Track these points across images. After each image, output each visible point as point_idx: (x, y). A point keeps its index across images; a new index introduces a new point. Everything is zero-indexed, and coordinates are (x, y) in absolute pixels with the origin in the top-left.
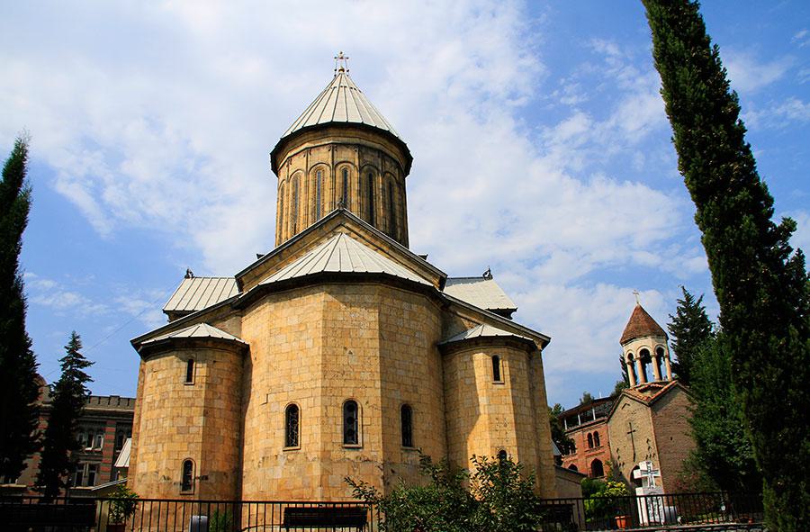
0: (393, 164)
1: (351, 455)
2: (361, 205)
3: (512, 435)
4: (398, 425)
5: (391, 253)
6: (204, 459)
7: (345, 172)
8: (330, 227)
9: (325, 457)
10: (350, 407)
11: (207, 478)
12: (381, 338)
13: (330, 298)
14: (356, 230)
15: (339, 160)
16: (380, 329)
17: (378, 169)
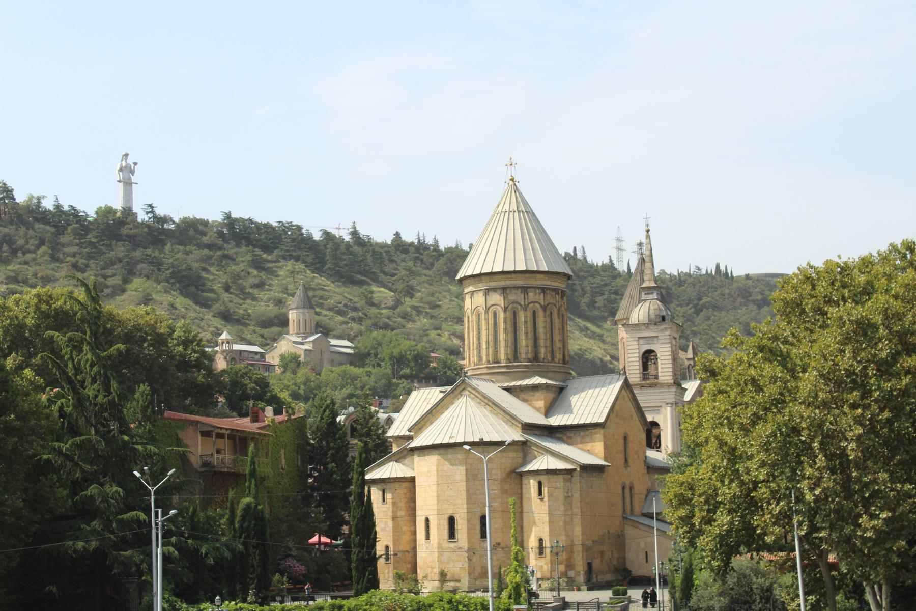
0: (538, 291)
1: (452, 545)
2: (506, 341)
3: (547, 529)
4: (478, 527)
5: (494, 407)
6: (394, 545)
7: (495, 314)
8: (458, 390)
9: (440, 547)
10: (452, 521)
11: (396, 554)
12: (468, 480)
13: (439, 457)
14: (474, 392)
15: (492, 303)
16: (467, 474)
17: (521, 305)
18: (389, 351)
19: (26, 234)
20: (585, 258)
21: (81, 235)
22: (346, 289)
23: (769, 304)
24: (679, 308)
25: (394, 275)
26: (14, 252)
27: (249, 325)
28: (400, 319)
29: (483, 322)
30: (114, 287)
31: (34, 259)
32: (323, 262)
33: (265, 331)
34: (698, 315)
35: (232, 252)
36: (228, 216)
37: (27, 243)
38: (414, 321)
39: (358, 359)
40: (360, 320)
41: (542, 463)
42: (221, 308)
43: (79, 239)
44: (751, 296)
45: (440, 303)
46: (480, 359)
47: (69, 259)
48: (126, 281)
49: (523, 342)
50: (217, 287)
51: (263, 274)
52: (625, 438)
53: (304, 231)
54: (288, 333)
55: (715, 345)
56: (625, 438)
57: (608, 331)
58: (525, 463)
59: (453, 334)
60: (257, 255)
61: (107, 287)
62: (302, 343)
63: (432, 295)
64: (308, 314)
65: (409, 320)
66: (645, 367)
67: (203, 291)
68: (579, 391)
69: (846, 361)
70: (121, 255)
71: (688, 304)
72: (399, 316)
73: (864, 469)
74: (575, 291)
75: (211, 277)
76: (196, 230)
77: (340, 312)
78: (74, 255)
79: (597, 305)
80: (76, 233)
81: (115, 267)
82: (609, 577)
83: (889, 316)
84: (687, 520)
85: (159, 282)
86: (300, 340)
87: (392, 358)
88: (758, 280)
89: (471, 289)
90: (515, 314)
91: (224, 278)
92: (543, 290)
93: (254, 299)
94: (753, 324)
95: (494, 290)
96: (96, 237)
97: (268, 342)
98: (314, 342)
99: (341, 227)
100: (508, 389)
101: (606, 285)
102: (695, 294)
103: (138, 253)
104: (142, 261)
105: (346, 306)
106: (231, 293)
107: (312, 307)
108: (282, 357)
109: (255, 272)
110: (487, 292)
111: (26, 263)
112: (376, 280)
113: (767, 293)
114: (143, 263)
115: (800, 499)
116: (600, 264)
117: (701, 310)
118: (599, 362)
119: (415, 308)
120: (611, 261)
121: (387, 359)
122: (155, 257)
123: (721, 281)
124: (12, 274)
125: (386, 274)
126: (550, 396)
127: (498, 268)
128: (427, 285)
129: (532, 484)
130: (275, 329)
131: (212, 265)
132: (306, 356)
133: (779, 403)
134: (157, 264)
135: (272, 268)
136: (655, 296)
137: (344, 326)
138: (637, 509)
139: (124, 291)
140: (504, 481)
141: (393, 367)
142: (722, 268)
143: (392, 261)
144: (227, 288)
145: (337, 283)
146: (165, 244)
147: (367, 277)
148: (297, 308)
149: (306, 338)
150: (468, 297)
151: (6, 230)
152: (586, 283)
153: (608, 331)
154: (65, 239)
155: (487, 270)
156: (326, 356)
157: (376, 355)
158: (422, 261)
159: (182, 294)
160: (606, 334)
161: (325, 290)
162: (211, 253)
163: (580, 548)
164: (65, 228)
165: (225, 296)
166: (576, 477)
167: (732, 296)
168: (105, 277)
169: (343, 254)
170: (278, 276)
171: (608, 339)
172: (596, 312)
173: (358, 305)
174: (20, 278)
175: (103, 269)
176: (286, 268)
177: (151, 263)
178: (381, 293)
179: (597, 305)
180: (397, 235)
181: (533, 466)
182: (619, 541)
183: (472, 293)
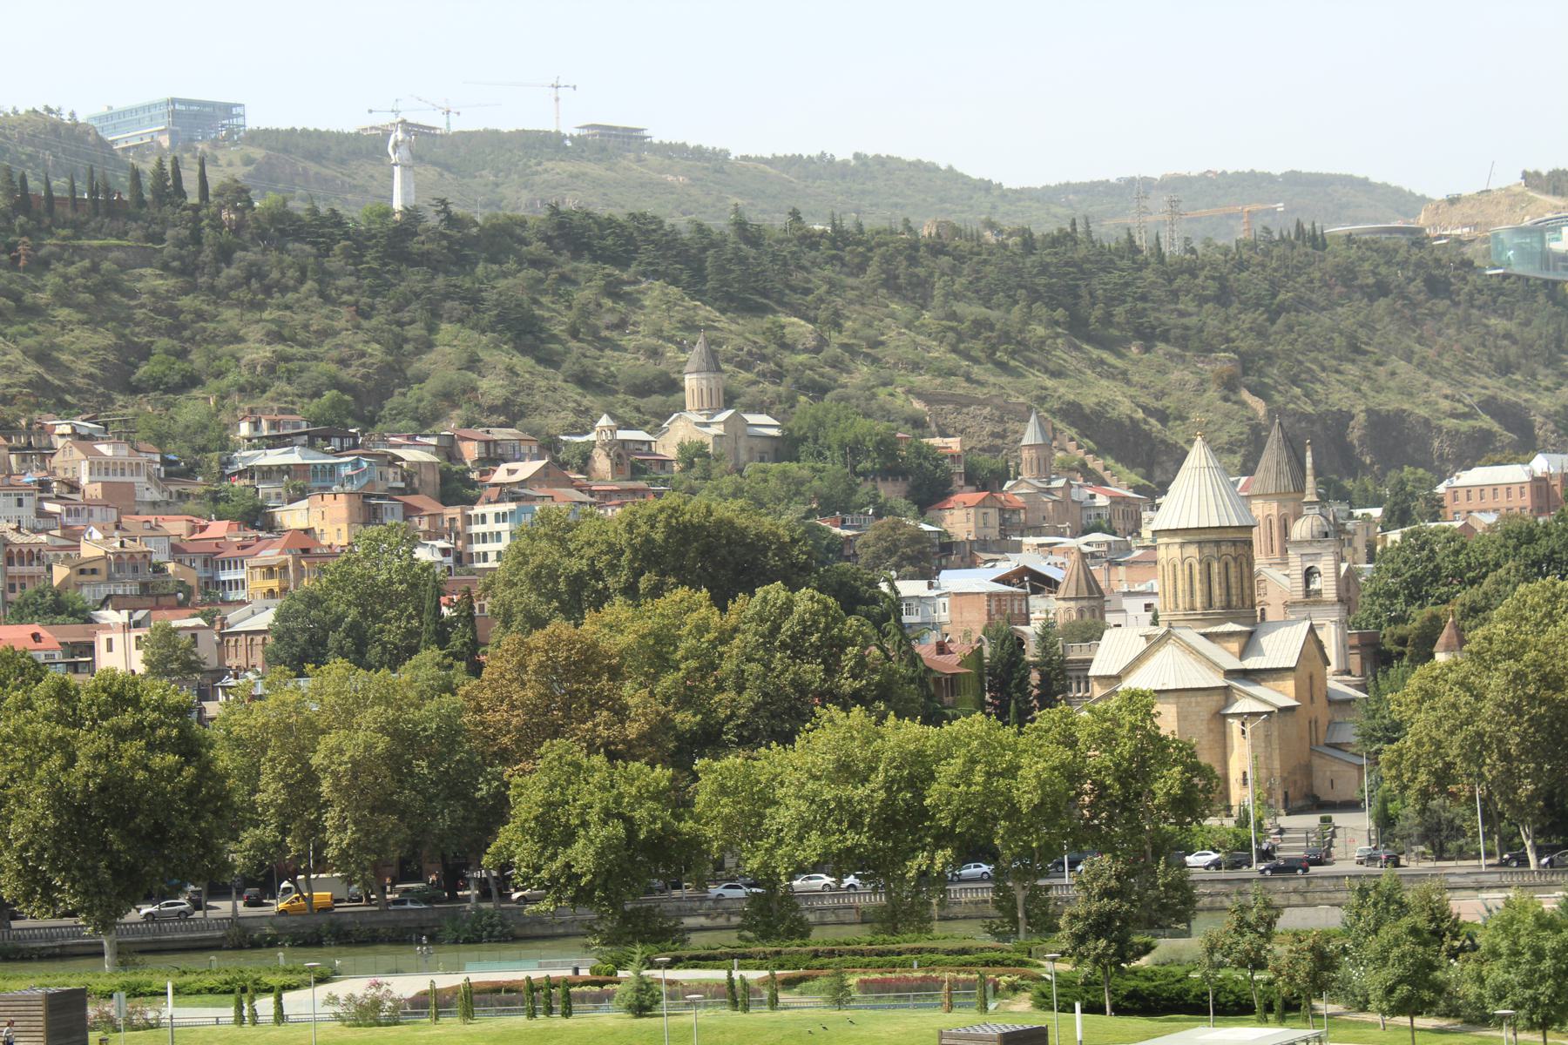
18: (838, 436)
19: (280, 261)
20: (1089, 233)
21: (354, 256)
22: (750, 326)
23: (1385, 295)
24: (1242, 316)
25: (807, 292)
26: (267, 291)
27: (617, 392)
28: (827, 369)
29: (1179, 573)
30: (415, 340)
31: (298, 300)
32: (699, 274)
33: (642, 402)
34: (1273, 322)
35: (567, 268)
36: (555, 210)
37: (283, 274)
38: (849, 372)
39: (786, 448)
40: (777, 376)
41: (1243, 706)
42: (576, 367)
43: (355, 264)
44: (1356, 278)
45: (883, 338)
46: (1177, 606)
47: (346, 298)
48: (432, 329)
49: (1216, 590)
50: (557, 330)
51: (621, 306)
52: (1311, 677)
53: (667, 227)
54: (683, 408)
55: (1303, 376)
56: (1311, 677)
57: (1135, 363)
58: (1227, 705)
59: (909, 391)
60: (609, 275)
61: (406, 340)
62: (707, 425)
63: (870, 326)
64: (716, 381)
65: (842, 370)
66: (1307, 583)
67: (543, 341)
68: (1267, 633)
69: (1508, 697)
70: (419, 287)
71: (1257, 305)
72: (826, 362)
73: (1522, 762)
74: (1078, 297)
75: (547, 314)
76: (512, 236)
77: (744, 365)
78: (350, 291)
79: (1116, 319)
80: (347, 253)
81: (412, 307)
82: (1300, 803)
83: (1537, 665)
84: (1399, 777)
85: (483, 332)
86: (703, 419)
87: (842, 445)
88: (1366, 242)
89: (1165, 540)
90: (1209, 565)
91: (569, 317)
92: (1234, 543)
93: (617, 347)
94: (1362, 334)
95: (1190, 543)
96: (375, 259)
97: (657, 420)
98: (725, 422)
99: (562, 83)
100: (1205, 635)
101: (1127, 284)
102: (1266, 285)
103: (440, 282)
104: (447, 296)
105: (750, 353)
106: (580, 341)
107: (719, 370)
108: (682, 448)
109: (608, 303)
110: (1182, 545)
111: (288, 307)
112: (780, 303)
113: (1383, 270)
114: (453, 299)
115: (1481, 776)
116: (1113, 245)
117: (1278, 314)
118: (1127, 422)
119: (844, 346)
120: (1130, 235)
121: (835, 447)
122: (468, 289)
123: (1306, 255)
124: (274, 327)
125: (794, 289)
126: (1243, 640)
127: (1194, 525)
128: (857, 307)
129: (1235, 725)
130: (656, 399)
131: (545, 292)
132: (715, 443)
133: (1468, 721)
134: (474, 300)
135: (629, 294)
136: (1317, 510)
137: (754, 389)
138: (1321, 741)
139: (430, 346)
140: (1210, 721)
141: (844, 456)
142: (1307, 227)
143: (803, 268)
144: (574, 333)
145: (729, 314)
146: (476, 264)
147: (767, 297)
148: (697, 372)
149: (713, 416)
150: (1162, 548)
151: (250, 256)
152: (1095, 282)
153: (1135, 363)
154: (334, 263)
155: (1183, 525)
156: (742, 443)
157: (816, 440)
158: (841, 259)
159: (515, 348)
160: (1132, 369)
161: (716, 329)
162: (541, 274)
163: (1278, 780)
164: (329, 249)
165: (574, 344)
166: (1274, 718)
167: (1327, 285)
168: (401, 324)
169: (730, 261)
170: (642, 307)
171: (1136, 378)
172: (1115, 332)
173: (765, 351)
174: (286, 333)
175: (395, 311)
176: (654, 292)
177: (463, 298)
178: (798, 328)
179: (1116, 319)
180: (795, 215)
181: (1235, 709)
182: (1307, 770)
183: (1168, 545)
